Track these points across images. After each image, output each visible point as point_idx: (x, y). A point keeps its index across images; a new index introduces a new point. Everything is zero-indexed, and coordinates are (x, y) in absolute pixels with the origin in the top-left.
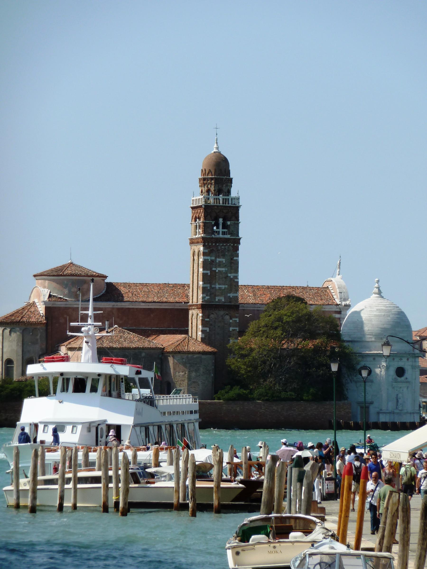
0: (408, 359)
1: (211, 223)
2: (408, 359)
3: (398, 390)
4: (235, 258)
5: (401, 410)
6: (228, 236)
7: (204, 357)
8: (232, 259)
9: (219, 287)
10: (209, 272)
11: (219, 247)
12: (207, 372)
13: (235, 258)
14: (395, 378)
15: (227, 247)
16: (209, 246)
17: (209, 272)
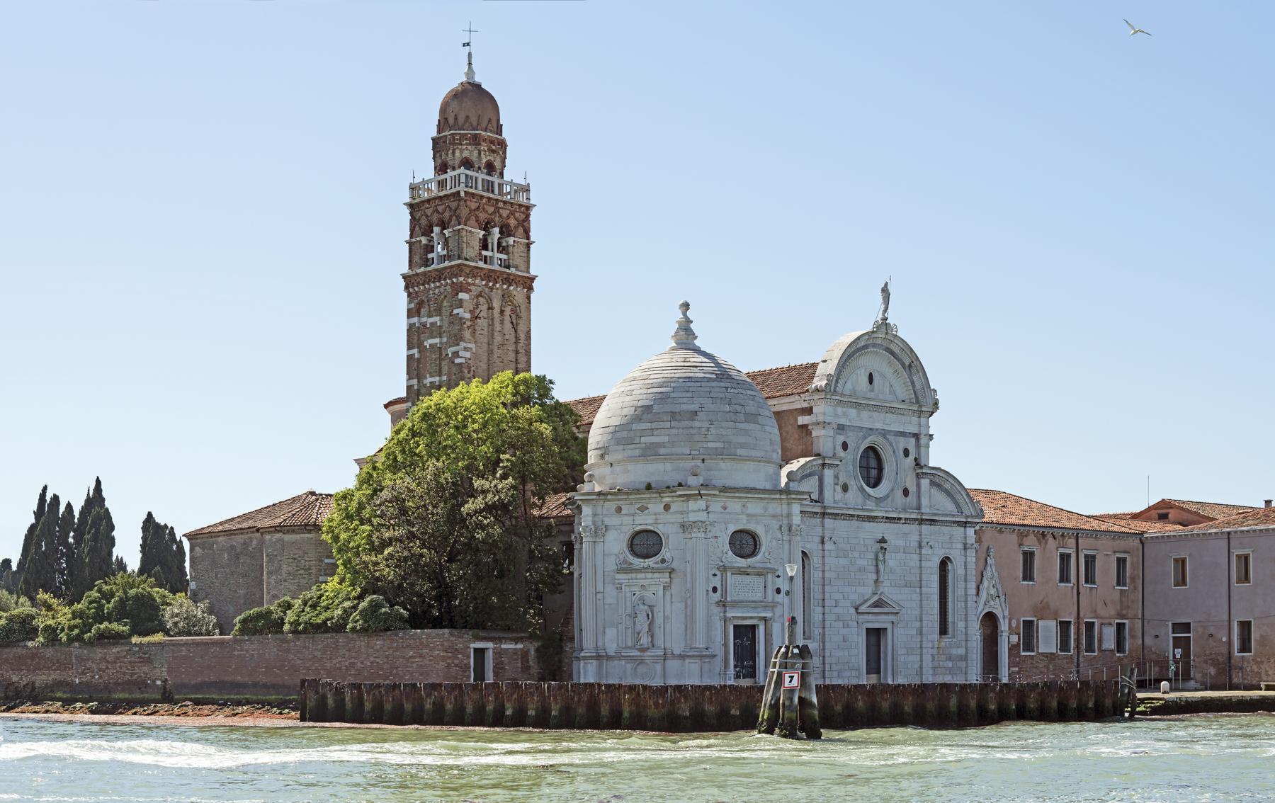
0: (667, 508)
1: (420, 241)
2: (667, 508)
3: (637, 593)
4: (455, 311)
5: (643, 650)
6: (447, 264)
7: (287, 537)
8: (451, 315)
9: (430, 383)
10: (415, 351)
11: (431, 292)
12: (302, 572)
13: (455, 311)
14: (625, 562)
15: (442, 289)
16: (416, 292)
17: (415, 351)
